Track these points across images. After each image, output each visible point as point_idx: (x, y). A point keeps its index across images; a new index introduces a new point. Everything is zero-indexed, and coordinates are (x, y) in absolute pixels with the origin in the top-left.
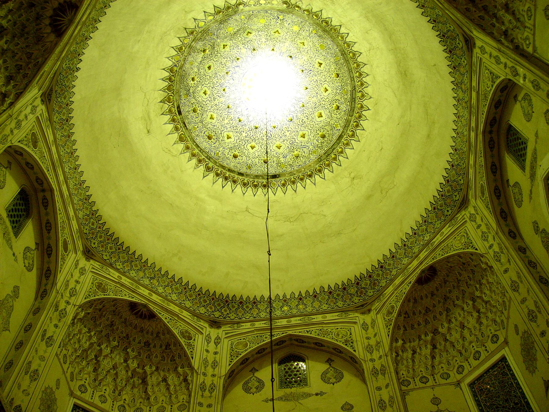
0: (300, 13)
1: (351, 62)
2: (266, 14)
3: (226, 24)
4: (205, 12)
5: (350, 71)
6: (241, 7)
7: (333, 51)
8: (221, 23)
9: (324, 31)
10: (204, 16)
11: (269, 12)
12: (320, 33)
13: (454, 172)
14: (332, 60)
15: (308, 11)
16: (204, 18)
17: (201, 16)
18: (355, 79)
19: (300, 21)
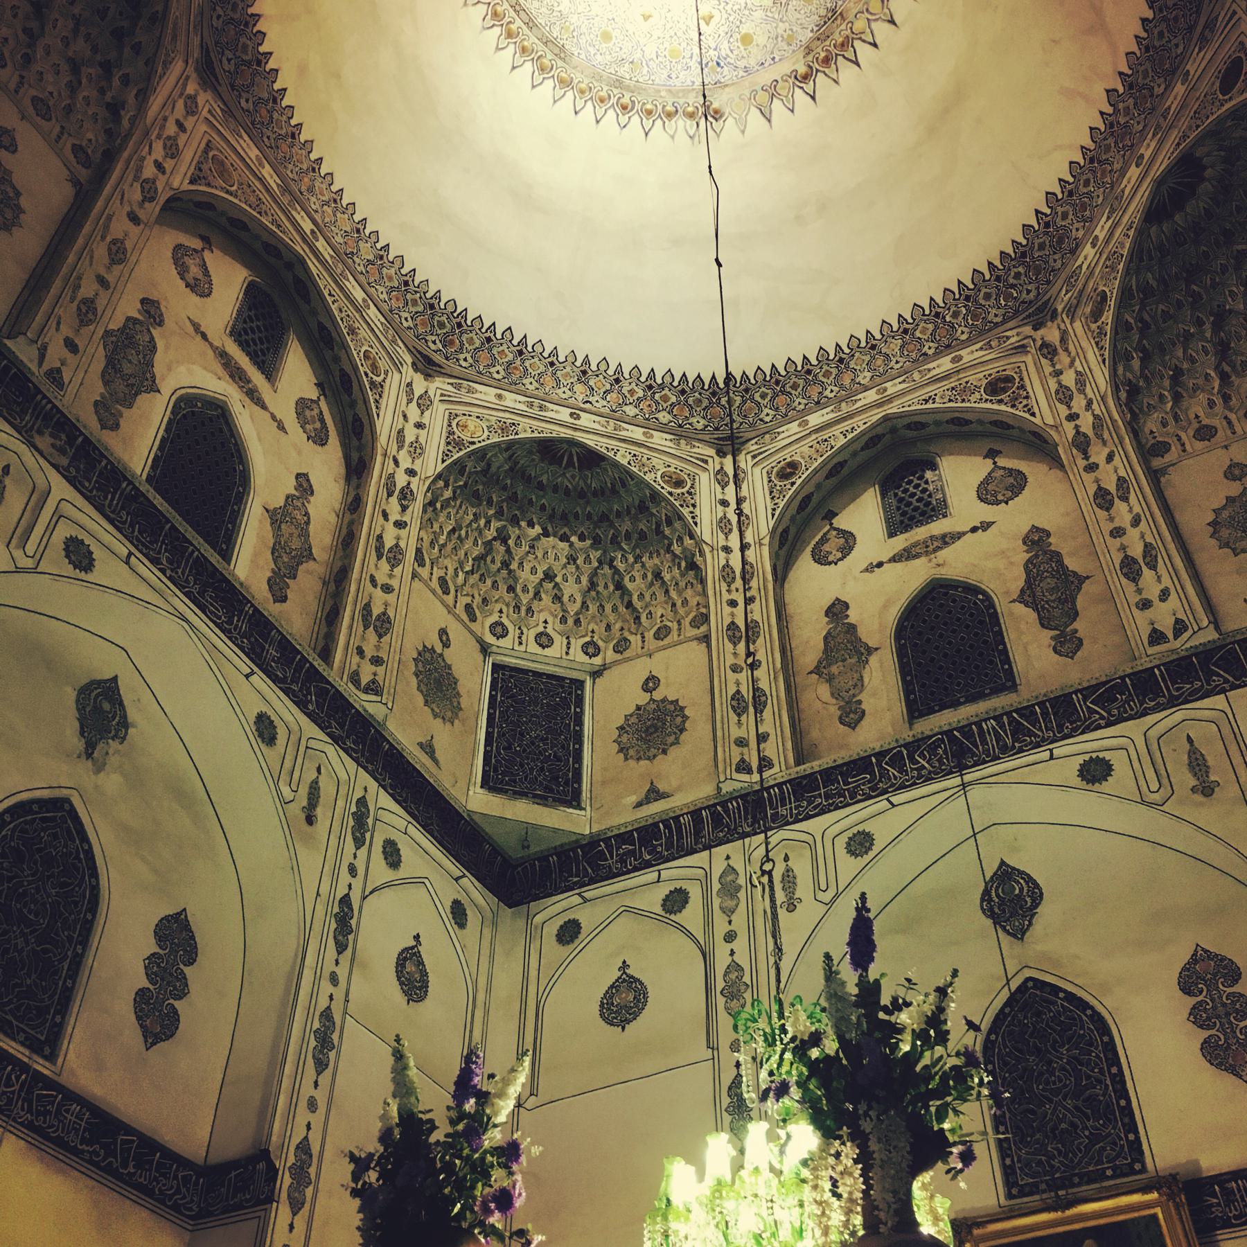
0: (681, 101)
1: (541, 47)
2: (741, 64)
3: (823, 12)
4: (875, 45)
5: (531, 24)
6: (802, 69)
7: (583, 41)
8: (834, 11)
9: (619, 83)
10: (875, 33)
11: (742, 73)
12: (624, 71)
13: (265, 96)
14: (574, 19)
15: (670, 115)
16: (873, 25)
17: (881, 30)
18: (513, 13)
19: (674, 76)
